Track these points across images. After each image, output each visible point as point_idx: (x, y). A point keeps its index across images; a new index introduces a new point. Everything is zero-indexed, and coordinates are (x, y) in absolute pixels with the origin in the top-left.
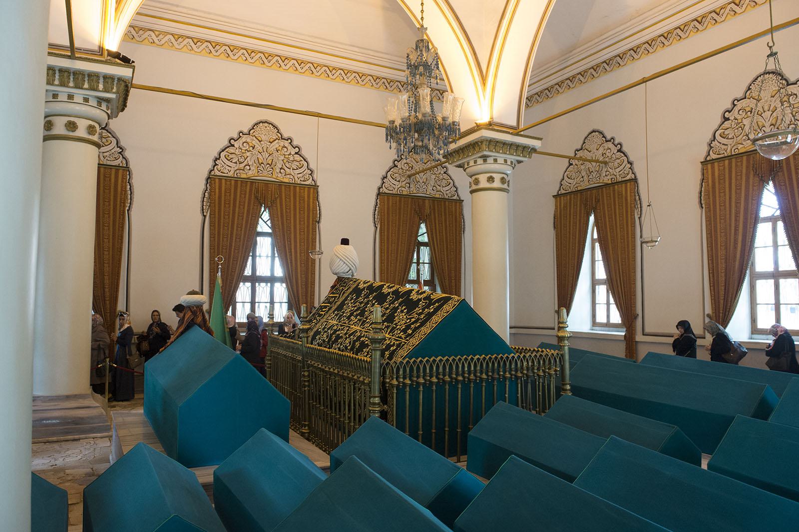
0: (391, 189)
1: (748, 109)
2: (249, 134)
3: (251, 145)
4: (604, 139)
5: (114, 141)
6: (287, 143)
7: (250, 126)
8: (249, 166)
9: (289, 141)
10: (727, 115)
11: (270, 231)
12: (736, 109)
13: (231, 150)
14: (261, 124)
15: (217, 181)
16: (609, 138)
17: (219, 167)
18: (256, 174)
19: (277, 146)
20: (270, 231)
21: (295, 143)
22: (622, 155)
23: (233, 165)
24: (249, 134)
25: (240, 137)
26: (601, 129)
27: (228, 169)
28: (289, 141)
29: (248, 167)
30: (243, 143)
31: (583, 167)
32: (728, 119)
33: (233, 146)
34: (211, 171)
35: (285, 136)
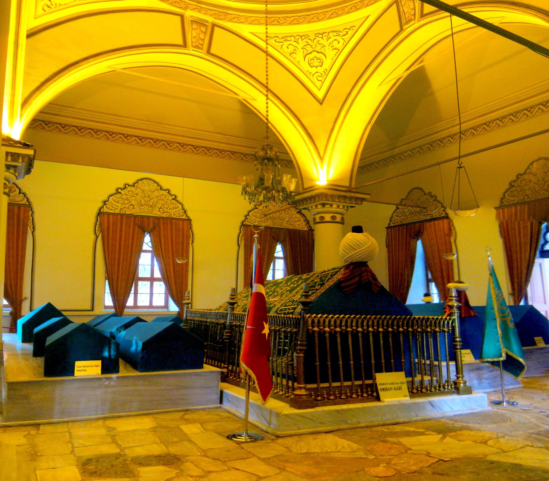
0: (251, 222)
1: (527, 180)
2: (134, 186)
3: (135, 192)
4: (423, 193)
5: (18, 190)
6: (165, 193)
7: (134, 180)
8: (133, 206)
9: (167, 191)
10: (513, 184)
11: (151, 249)
12: (519, 181)
13: (118, 195)
14: (144, 180)
15: (106, 216)
16: (427, 192)
17: (108, 205)
18: (139, 211)
19: (157, 194)
20: (151, 249)
21: (172, 193)
22: (437, 202)
23: (119, 205)
24: (134, 186)
25: (126, 187)
26: (420, 186)
27: (115, 207)
29: (132, 207)
30: (129, 191)
31: (406, 210)
32: (514, 186)
33: (120, 193)
34: (101, 208)
35: (165, 187)
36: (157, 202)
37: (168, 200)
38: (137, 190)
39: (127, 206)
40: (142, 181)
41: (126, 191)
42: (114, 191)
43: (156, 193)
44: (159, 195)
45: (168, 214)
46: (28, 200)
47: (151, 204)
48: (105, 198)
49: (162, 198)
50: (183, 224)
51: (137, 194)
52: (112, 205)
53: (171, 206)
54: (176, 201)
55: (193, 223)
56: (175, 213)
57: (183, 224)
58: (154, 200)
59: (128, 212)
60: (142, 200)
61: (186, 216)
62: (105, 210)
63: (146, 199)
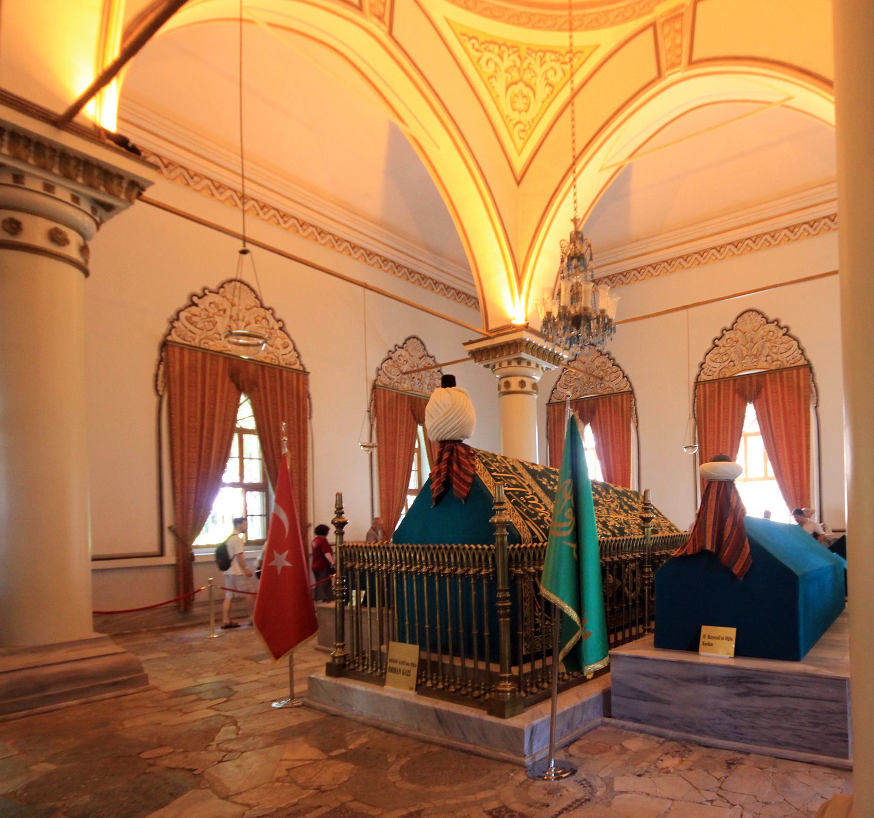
9: (776, 323)
17: (705, 370)
23: (717, 365)
24: (732, 329)
27: (714, 371)
28: (776, 323)
29: (732, 364)
36: (763, 347)
37: (777, 338)
38: (736, 334)
39: (726, 363)
40: (742, 317)
41: (724, 340)
42: (709, 345)
43: (761, 332)
44: (765, 334)
45: (779, 363)
46: (631, 386)
47: (755, 353)
48: (701, 360)
49: (769, 337)
50: (798, 374)
51: (737, 342)
52: (710, 368)
53: (783, 348)
54: (790, 336)
55: (816, 370)
56: (788, 359)
57: (798, 374)
58: (758, 344)
59: (728, 375)
60: (744, 349)
61: (805, 359)
62: (703, 377)
63: (748, 346)
